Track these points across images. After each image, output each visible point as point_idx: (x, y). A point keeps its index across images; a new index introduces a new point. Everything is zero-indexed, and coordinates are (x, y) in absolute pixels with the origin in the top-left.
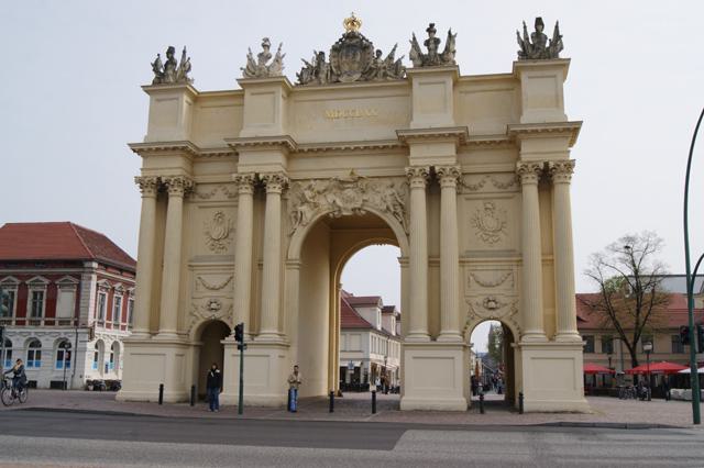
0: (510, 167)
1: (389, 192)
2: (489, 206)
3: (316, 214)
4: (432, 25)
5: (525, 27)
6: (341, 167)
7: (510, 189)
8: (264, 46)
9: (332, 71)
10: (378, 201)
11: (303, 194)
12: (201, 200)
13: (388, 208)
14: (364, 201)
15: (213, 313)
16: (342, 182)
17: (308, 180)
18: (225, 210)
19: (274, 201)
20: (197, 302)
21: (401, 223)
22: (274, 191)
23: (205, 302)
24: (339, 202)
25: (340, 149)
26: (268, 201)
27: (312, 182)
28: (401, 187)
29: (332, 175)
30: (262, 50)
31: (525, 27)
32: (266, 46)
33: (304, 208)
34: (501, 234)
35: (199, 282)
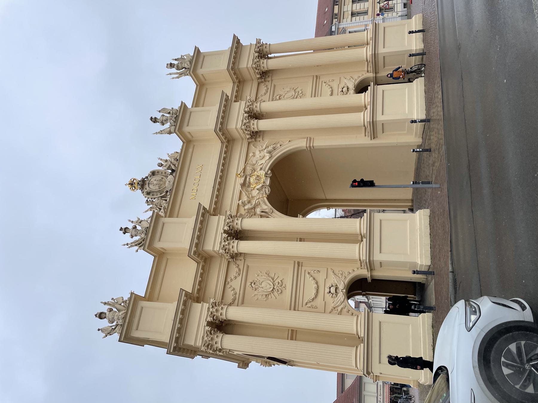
1: (257, 153)
2: (278, 97)
3: (264, 202)
4: (151, 118)
5: (170, 74)
9: (162, 197)
10: (263, 161)
12: (237, 301)
14: (261, 169)
18: (250, 280)
20: (329, 309)
23: (329, 297)
24: (259, 186)
28: (256, 147)
29: (238, 188)
30: (128, 235)
31: (170, 74)
32: (125, 231)
34: (297, 90)
35: (309, 305)
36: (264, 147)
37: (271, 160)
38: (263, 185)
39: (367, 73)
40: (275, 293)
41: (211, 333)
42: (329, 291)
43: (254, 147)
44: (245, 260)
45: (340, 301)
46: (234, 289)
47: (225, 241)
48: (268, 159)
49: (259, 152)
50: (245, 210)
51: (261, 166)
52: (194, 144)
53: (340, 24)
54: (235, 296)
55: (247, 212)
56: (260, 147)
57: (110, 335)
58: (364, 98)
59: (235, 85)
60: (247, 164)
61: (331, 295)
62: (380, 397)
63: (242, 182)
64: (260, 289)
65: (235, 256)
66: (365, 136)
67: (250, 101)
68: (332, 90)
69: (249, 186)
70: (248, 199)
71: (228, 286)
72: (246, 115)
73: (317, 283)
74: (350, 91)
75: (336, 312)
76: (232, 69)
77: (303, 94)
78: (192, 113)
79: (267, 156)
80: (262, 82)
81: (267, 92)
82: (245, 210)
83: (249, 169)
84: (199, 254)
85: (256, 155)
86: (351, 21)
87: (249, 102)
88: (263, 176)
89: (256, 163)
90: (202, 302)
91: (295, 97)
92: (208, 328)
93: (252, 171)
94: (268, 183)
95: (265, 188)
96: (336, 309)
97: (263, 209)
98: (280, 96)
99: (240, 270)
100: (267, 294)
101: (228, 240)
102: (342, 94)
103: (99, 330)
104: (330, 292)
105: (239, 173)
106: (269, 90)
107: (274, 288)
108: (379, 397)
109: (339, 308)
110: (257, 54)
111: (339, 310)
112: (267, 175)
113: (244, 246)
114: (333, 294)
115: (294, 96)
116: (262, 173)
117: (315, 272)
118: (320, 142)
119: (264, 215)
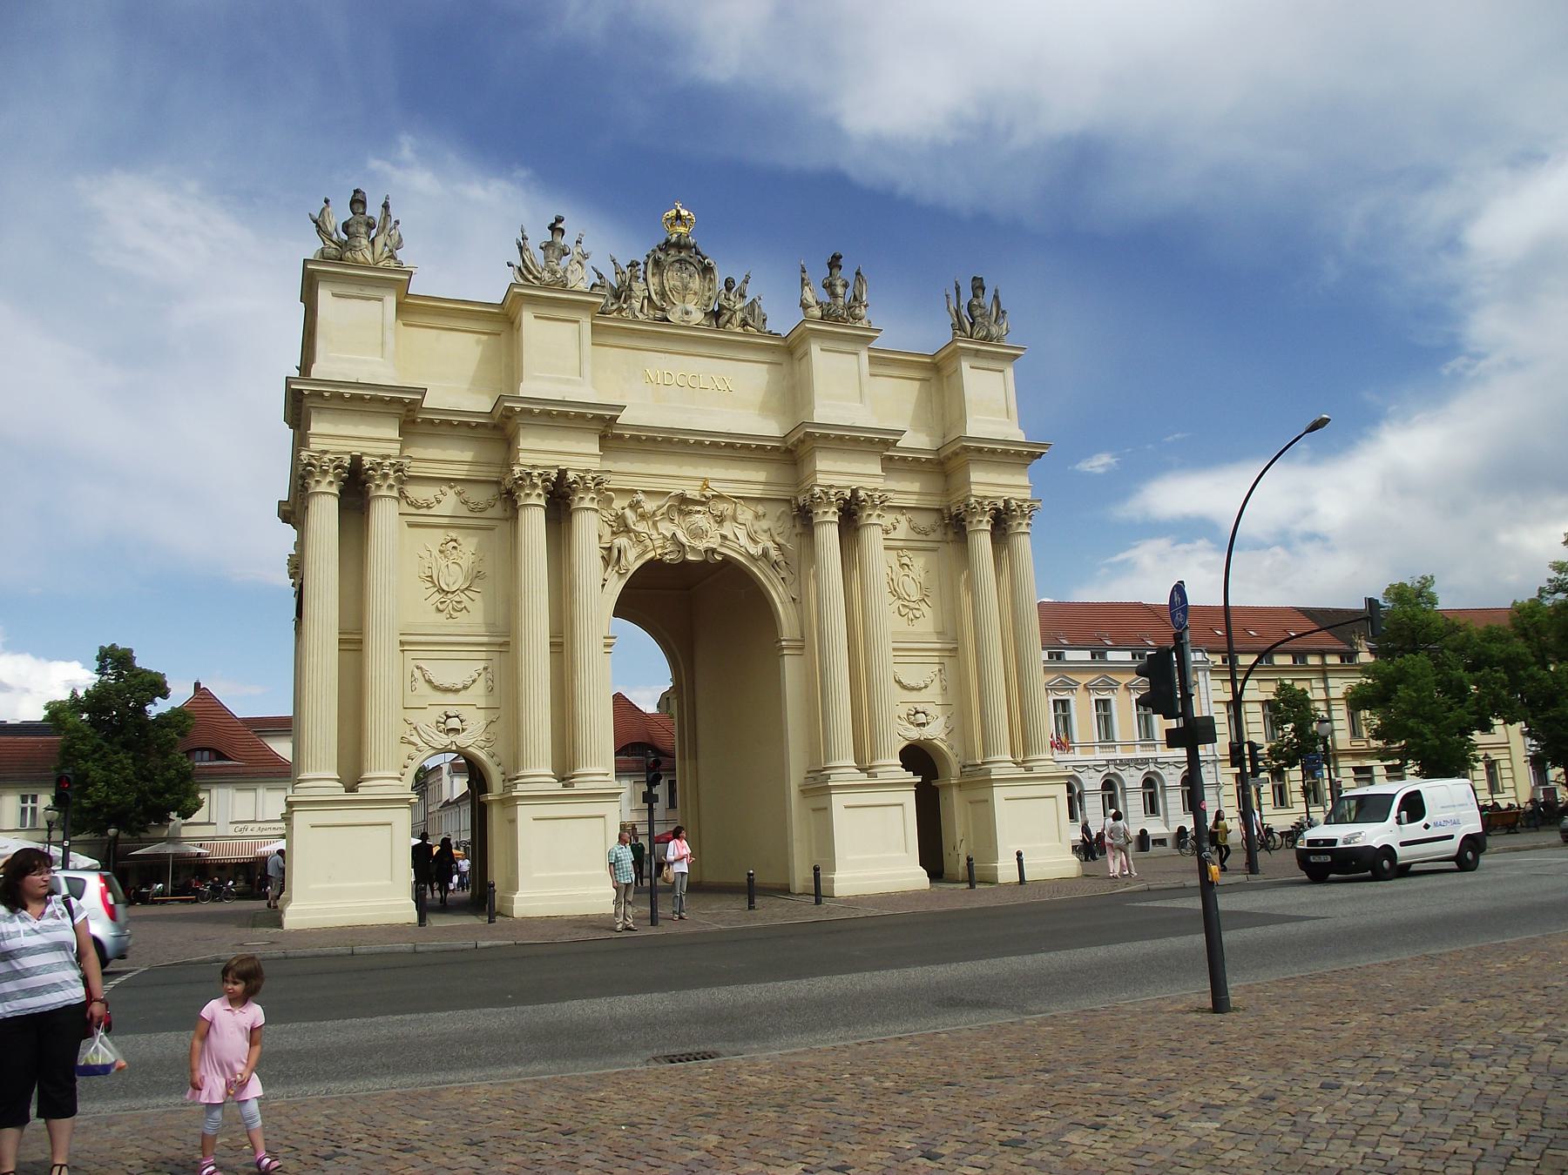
0: (933, 502)
1: (765, 524)
2: (905, 560)
3: (644, 552)
5: (958, 289)
6: (686, 476)
7: (932, 536)
8: (553, 228)
9: (649, 298)
10: (744, 540)
11: (621, 518)
13: (765, 554)
14: (724, 537)
15: (453, 737)
16: (683, 500)
17: (635, 492)
19: (589, 528)
20: (413, 716)
21: (782, 578)
22: (585, 500)
23: (437, 713)
25: (685, 442)
26: (574, 521)
27: (641, 497)
28: (779, 518)
29: (676, 488)
30: (548, 236)
31: (958, 289)
33: (622, 541)
35: (417, 673)
36: (778, 539)
37: (748, 559)
38: (683, 546)
39: (960, 765)
40: (437, 596)
41: (336, 468)
42: (451, 715)
43: (778, 514)
44: (507, 520)
45: (431, 739)
46: (439, 502)
47: (540, 475)
48: (749, 553)
49: (765, 527)
50: (623, 509)
51: (731, 536)
52: (784, 365)
53: (1208, 673)
54: (424, 507)
55: (617, 514)
56: (781, 530)
57: (318, 232)
58: (891, 765)
59: (930, 454)
60: (736, 503)
61: (443, 721)
62: (256, 829)
63: (688, 496)
64: (443, 562)
65: (509, 499)
66: (809, 772)
67: (883, 499)
68: (920, 689)
69: (681, 512)
70: (649, 513)
71: (444, 488)
72: (848, 493)
73: (465, 688)
74: (918, 728)
75: (408, 732)
76: (966, 448)
77: (912, 620)
78: (854, 356)
79: (755, 550)
80: (943, 518)
81: (919, 533)
82: (623, 509)
83: (722, 507)
84: (508, 418)
85: (759, 521)
86: (1215, 702)
87: (880, 497)
88: (706, 545)
89: (740, 524)
90: (401, 439)
91: (906, 603)
92: (347, 461)
93: (719, 517)
94: (690, 558)
95: (679, 552)
96: (414, 732)
97: (625, 550)
98: (908, 566)
99: (482, 510)
100: (432, 578)
101: (544, 481)
102: (911, 712)
103: (327, 201)
104: (448, 717)
105: (710, 485)
106: (925, 538)
107: (448, 592)
108: (256, 826)
109: (415, 739)
110: (1001, 505)
111: (412, 739)
112: (709, 553)
113: (534, 521)
114: (444, 723)
115: (908, 598)
116: (712, 540)
117: (490, 682)
118: (791, 667)
119: (610, 557)
